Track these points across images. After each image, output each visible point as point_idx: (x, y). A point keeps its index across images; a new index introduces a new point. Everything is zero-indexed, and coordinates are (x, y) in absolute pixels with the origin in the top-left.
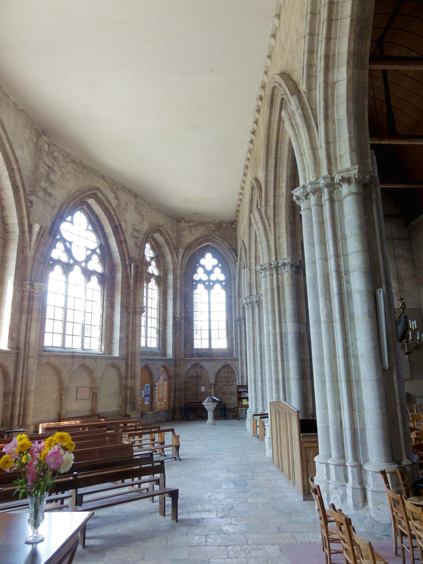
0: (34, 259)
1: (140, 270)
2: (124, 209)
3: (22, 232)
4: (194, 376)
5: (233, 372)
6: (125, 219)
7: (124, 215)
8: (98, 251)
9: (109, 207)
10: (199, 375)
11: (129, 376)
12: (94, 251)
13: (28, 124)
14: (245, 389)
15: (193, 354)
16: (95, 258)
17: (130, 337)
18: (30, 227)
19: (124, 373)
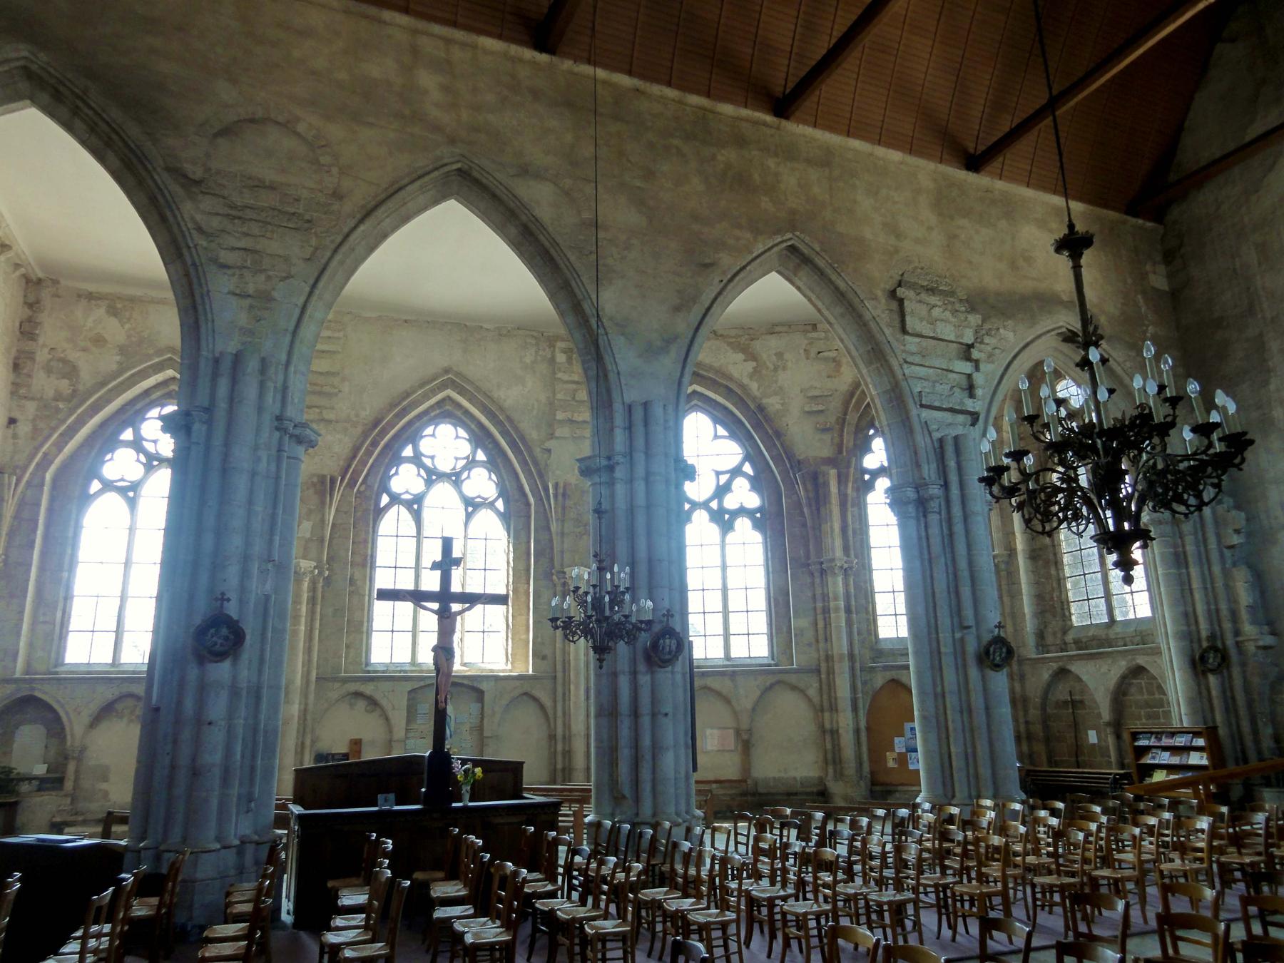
0: (563, 534)
1: (821, 480)
2: (776, 369)
3: (539, 500)
4: (1066, 702)
5: (1160, 687)
6: (781, 388)
7: (776, 382)
8: (748, 468)
9: (728, 384)
10: (1077, 698)
11: (826, 704)
12: (736, 472)
13: (529, 340)
14: (1153, 739)
15: (1065, 643)
16: (741, 485)
17: (821, 624)
18: (546, 489)
19: (816, 700)
